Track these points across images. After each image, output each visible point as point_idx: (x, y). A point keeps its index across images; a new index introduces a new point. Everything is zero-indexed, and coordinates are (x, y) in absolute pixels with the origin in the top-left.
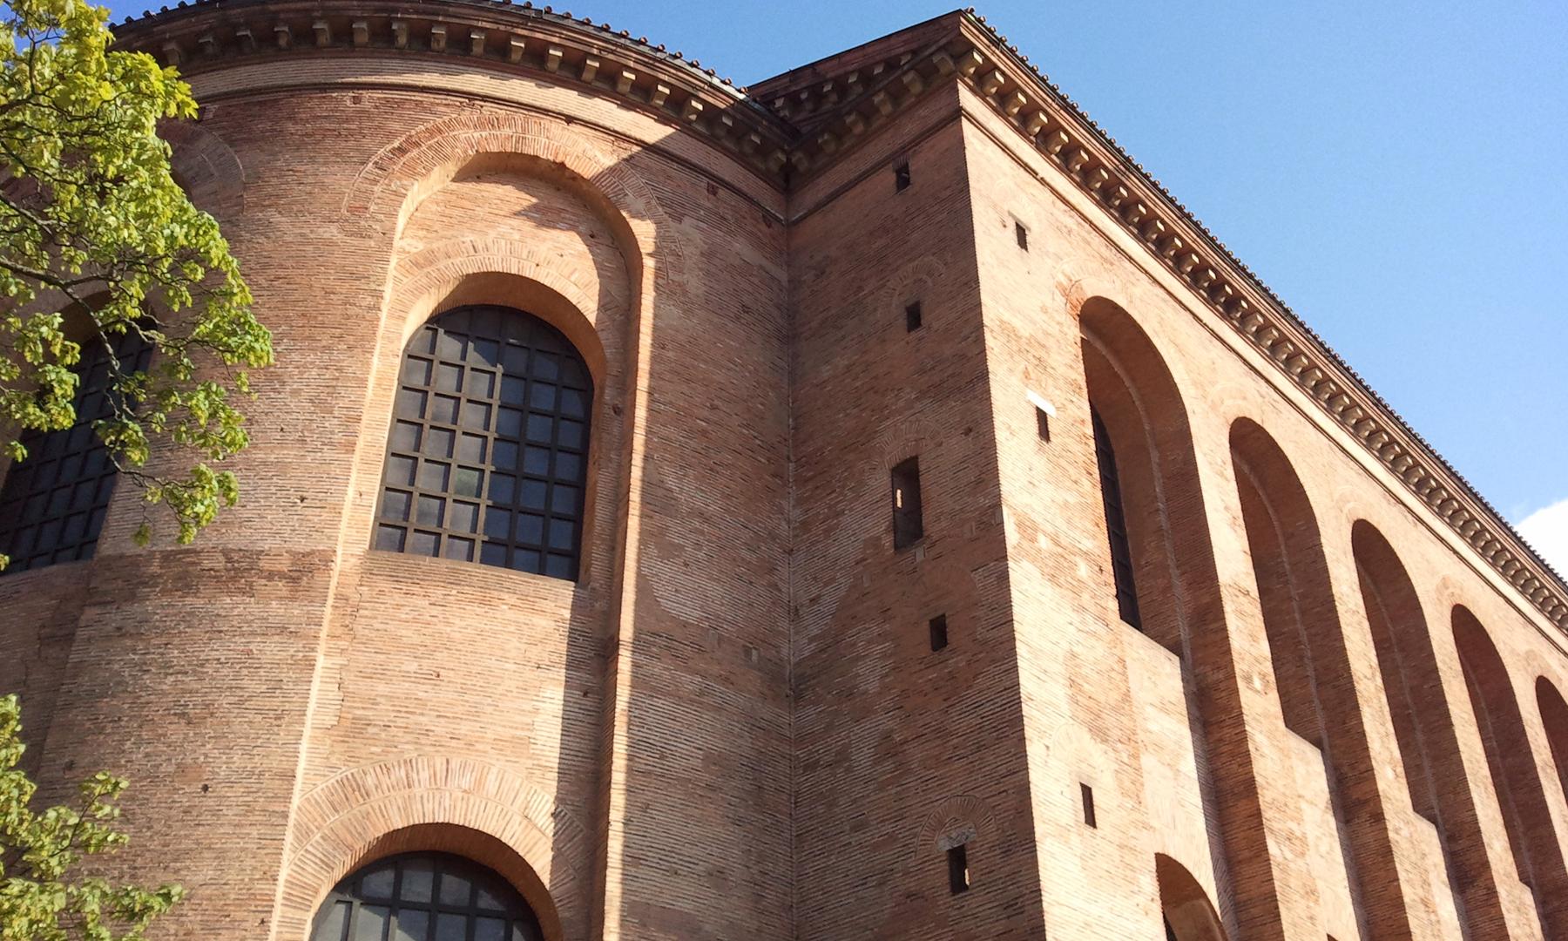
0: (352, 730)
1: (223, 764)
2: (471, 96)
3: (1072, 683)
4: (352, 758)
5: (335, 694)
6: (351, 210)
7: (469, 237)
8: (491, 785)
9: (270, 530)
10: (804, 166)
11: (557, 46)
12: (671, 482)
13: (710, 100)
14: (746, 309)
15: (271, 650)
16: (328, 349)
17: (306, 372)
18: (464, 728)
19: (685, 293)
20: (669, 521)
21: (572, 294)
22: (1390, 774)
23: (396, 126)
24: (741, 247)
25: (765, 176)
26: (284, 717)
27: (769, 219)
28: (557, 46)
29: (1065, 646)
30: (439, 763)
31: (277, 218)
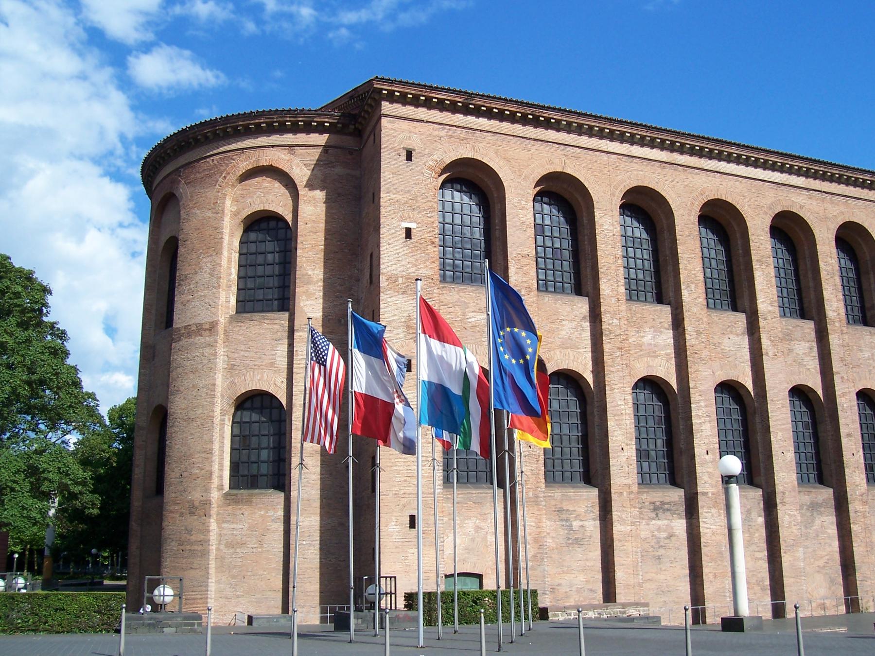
0: (231, 368)
1: (201, 383)
2: (242, 149)
3: (408, 327)
4: (232, 376)
5: (226, 359)
6: (214, 203)
7: (249, 200)
8: (265, 378)
9: (203, 317)
10: (360, 128)
11: (263, 123)
12: (310, 272)
13: (319, 120)
14: (339, 194)
15: (207, 351)
16: (211, 255)
17: (206, 264)
18: (257, 363)
19: (314, 199)
20: (310, 286)
21: (280, 211)
22: (614, 301)
23: (223, 168)
24: (339, 170)
25: (350, 134)
26: (212, 369)
27: (351, 153)
28: (263, 123)
29: (406, 315)
30: (252, 373)
31: (198, 212)
